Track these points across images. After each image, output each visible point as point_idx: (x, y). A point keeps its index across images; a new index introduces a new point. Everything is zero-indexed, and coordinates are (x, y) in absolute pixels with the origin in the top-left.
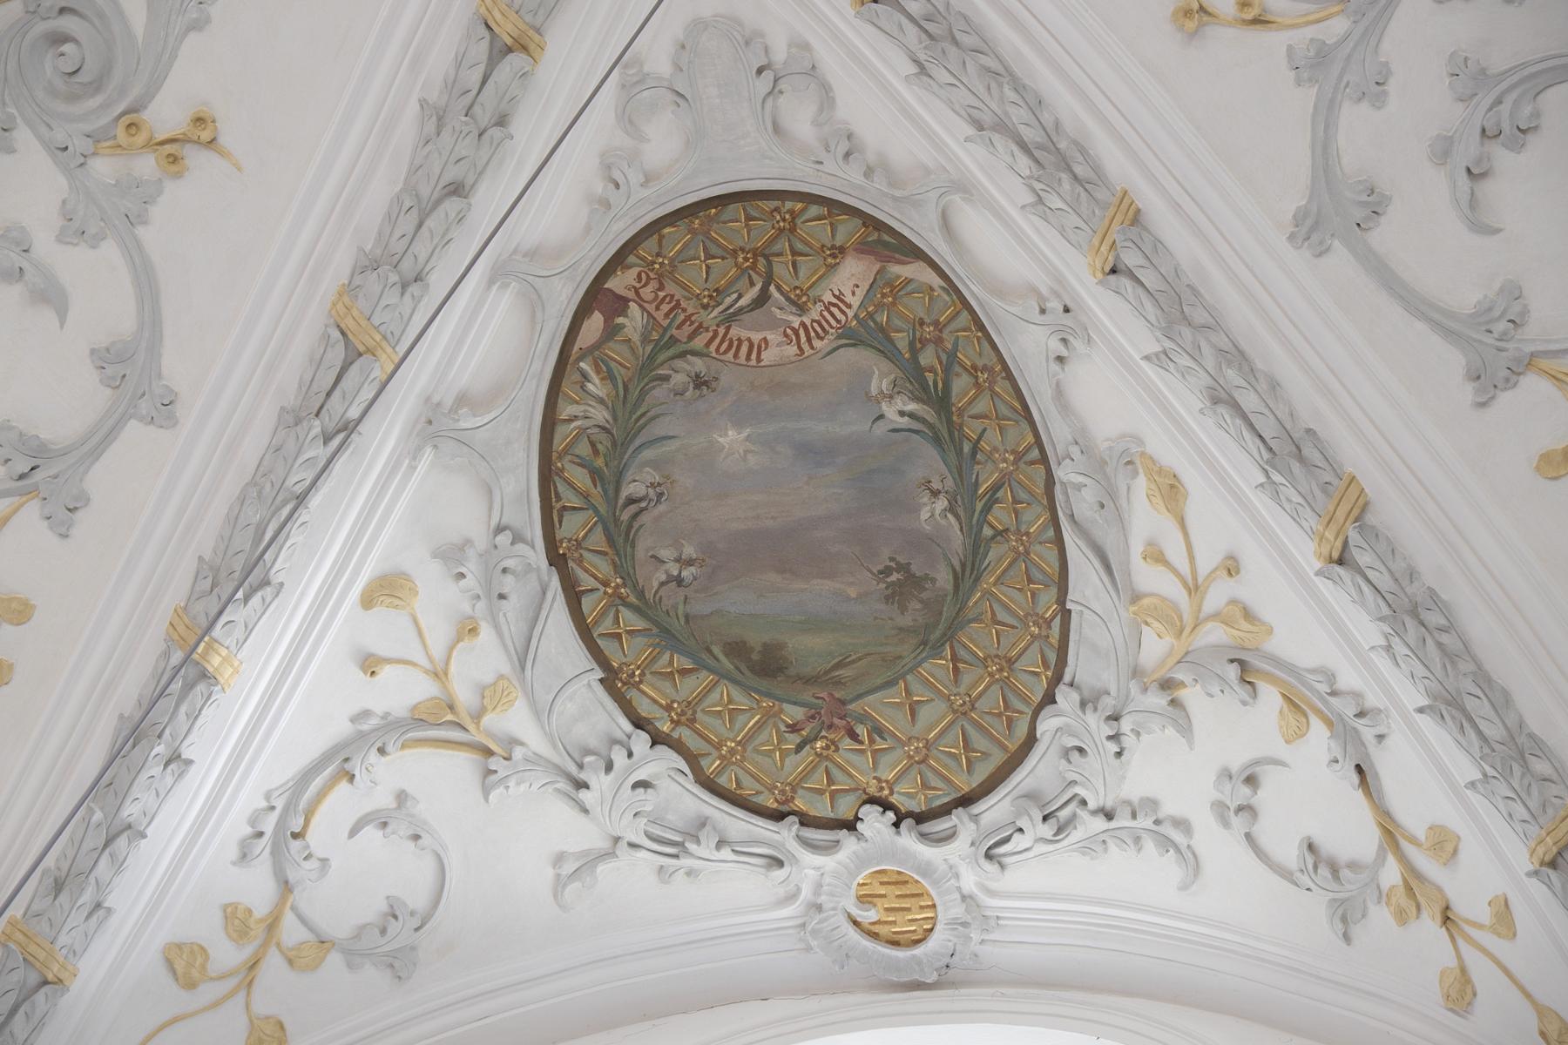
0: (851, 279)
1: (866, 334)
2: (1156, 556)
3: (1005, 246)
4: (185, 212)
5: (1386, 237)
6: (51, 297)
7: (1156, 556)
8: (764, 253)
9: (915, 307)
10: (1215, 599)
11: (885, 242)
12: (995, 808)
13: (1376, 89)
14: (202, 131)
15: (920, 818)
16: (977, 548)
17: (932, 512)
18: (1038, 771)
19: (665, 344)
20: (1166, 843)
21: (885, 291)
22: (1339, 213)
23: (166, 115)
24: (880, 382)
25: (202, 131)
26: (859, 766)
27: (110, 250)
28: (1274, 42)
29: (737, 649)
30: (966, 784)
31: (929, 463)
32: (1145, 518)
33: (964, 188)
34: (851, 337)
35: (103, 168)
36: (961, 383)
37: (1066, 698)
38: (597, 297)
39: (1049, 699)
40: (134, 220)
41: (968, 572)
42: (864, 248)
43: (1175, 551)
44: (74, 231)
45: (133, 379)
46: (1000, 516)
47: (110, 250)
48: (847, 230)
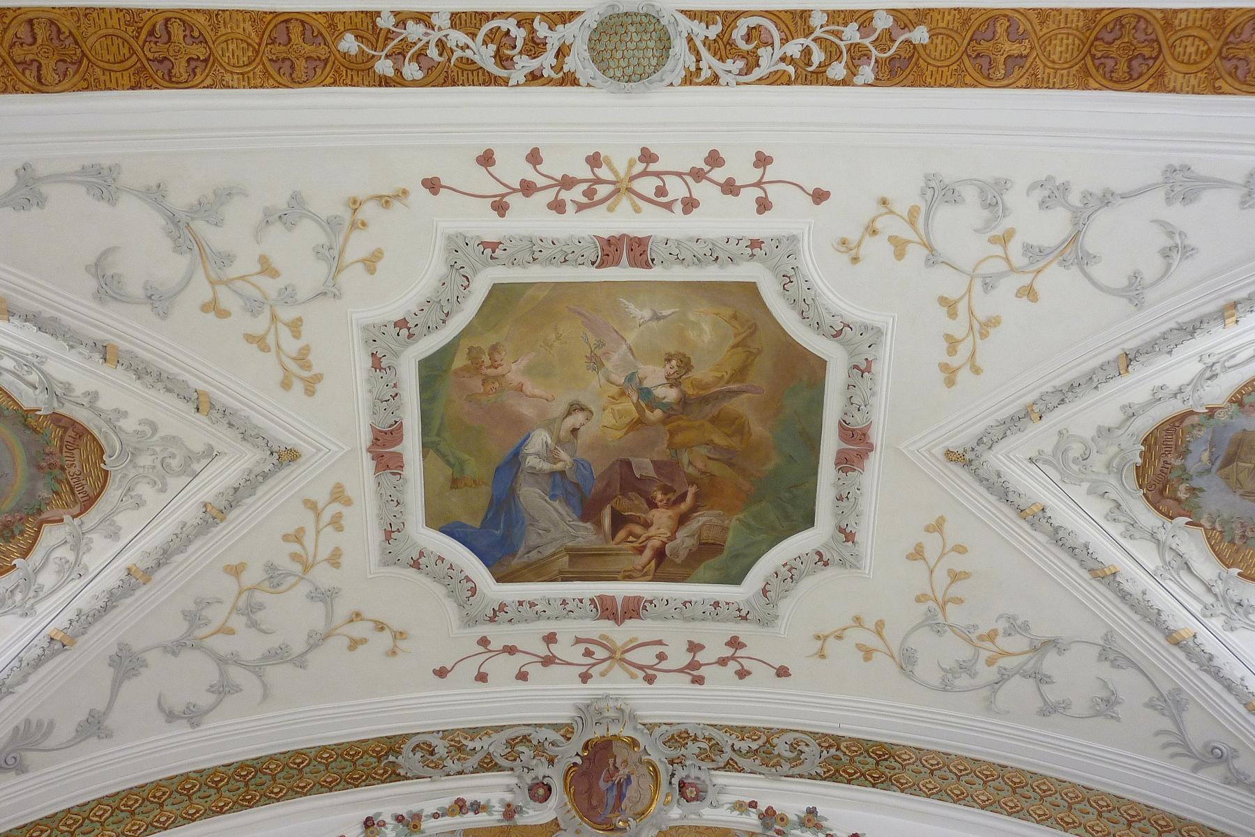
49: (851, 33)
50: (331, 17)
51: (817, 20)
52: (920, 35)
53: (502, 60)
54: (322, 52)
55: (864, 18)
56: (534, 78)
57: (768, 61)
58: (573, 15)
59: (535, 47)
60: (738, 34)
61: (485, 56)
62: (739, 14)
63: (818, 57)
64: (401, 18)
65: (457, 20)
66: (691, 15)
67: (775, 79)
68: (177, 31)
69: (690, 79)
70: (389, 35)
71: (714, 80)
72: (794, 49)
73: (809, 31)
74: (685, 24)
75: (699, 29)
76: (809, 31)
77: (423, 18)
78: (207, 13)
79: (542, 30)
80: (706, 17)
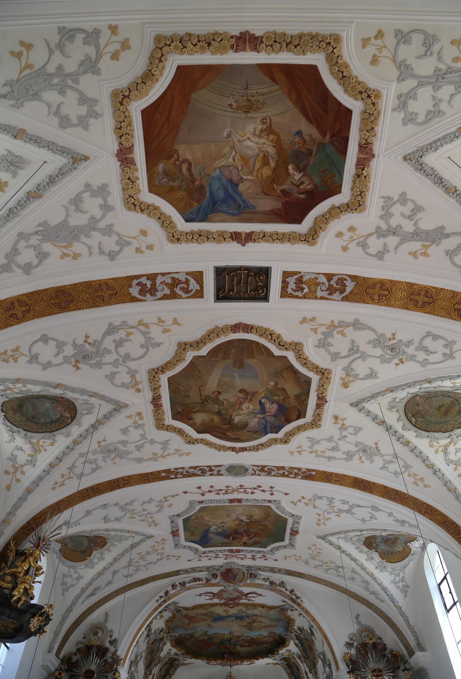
0: (67, 415)
1: (62, 416)
2: (44, 442)
3: (75, 430)
4: (69, 368)
6: (56, 355)
7: (44, 442)
8: (69, 408)
9: (66, 420)
10: (41, 448)
11: (73, 418)
12: (9, 424)
14: (78, 368)
15: (5, 417)
16: (40, 424)
17: (43, 420)
18: (15, 428)
19: (58, 401)
20: (11, 440)
21: (67, 418)
22: (81, 455)
23: (80, 365)
24: (57, 417)
25: (78, 368)
26: (10, 412)
27: (63, 361)
28: (97, 448)
29: (22, 404)
30: (11, 421)
31: (49, 420)
32: (48, 441)
33: (80, 427)
34: (61, 415)
35: (73, 360)
36: (58, 424)
37: (25, 432)
38: (62, 398)
39: (24, 430)
40: (67, 363)
41: (37, 423)
42: (71, 416)
43: (45, 444)
44: (65, 357)
45: (47, 365)
46: (44, 427)
47: (63, 361)
48: (74, 415)
49: (296, 471)
50: (159, 472)
51: (286, 468)
52: (314, 473)
53: (202, 472)
54: (157, 477)
55: (299, 469)
56: (211, 475)
57: (273, 473)
58: (221, 466)
59: (211, 470)
60: (266, 469)
61: (199, 473)
62: (266, 466)
63: (286, 473)
64: (176, 469)
65: (190, 468)
66: (254, 466)
68: (121, 481)
69: (252, 474)
70: (173, 472)
71: (259, 475)
72: (281, 472)
73: (284, 469)
74: (252, 467)
75: (255, 468)
76: (284, 469)
77: (183, 468)
79: (213, 468)
80: (258, 466)
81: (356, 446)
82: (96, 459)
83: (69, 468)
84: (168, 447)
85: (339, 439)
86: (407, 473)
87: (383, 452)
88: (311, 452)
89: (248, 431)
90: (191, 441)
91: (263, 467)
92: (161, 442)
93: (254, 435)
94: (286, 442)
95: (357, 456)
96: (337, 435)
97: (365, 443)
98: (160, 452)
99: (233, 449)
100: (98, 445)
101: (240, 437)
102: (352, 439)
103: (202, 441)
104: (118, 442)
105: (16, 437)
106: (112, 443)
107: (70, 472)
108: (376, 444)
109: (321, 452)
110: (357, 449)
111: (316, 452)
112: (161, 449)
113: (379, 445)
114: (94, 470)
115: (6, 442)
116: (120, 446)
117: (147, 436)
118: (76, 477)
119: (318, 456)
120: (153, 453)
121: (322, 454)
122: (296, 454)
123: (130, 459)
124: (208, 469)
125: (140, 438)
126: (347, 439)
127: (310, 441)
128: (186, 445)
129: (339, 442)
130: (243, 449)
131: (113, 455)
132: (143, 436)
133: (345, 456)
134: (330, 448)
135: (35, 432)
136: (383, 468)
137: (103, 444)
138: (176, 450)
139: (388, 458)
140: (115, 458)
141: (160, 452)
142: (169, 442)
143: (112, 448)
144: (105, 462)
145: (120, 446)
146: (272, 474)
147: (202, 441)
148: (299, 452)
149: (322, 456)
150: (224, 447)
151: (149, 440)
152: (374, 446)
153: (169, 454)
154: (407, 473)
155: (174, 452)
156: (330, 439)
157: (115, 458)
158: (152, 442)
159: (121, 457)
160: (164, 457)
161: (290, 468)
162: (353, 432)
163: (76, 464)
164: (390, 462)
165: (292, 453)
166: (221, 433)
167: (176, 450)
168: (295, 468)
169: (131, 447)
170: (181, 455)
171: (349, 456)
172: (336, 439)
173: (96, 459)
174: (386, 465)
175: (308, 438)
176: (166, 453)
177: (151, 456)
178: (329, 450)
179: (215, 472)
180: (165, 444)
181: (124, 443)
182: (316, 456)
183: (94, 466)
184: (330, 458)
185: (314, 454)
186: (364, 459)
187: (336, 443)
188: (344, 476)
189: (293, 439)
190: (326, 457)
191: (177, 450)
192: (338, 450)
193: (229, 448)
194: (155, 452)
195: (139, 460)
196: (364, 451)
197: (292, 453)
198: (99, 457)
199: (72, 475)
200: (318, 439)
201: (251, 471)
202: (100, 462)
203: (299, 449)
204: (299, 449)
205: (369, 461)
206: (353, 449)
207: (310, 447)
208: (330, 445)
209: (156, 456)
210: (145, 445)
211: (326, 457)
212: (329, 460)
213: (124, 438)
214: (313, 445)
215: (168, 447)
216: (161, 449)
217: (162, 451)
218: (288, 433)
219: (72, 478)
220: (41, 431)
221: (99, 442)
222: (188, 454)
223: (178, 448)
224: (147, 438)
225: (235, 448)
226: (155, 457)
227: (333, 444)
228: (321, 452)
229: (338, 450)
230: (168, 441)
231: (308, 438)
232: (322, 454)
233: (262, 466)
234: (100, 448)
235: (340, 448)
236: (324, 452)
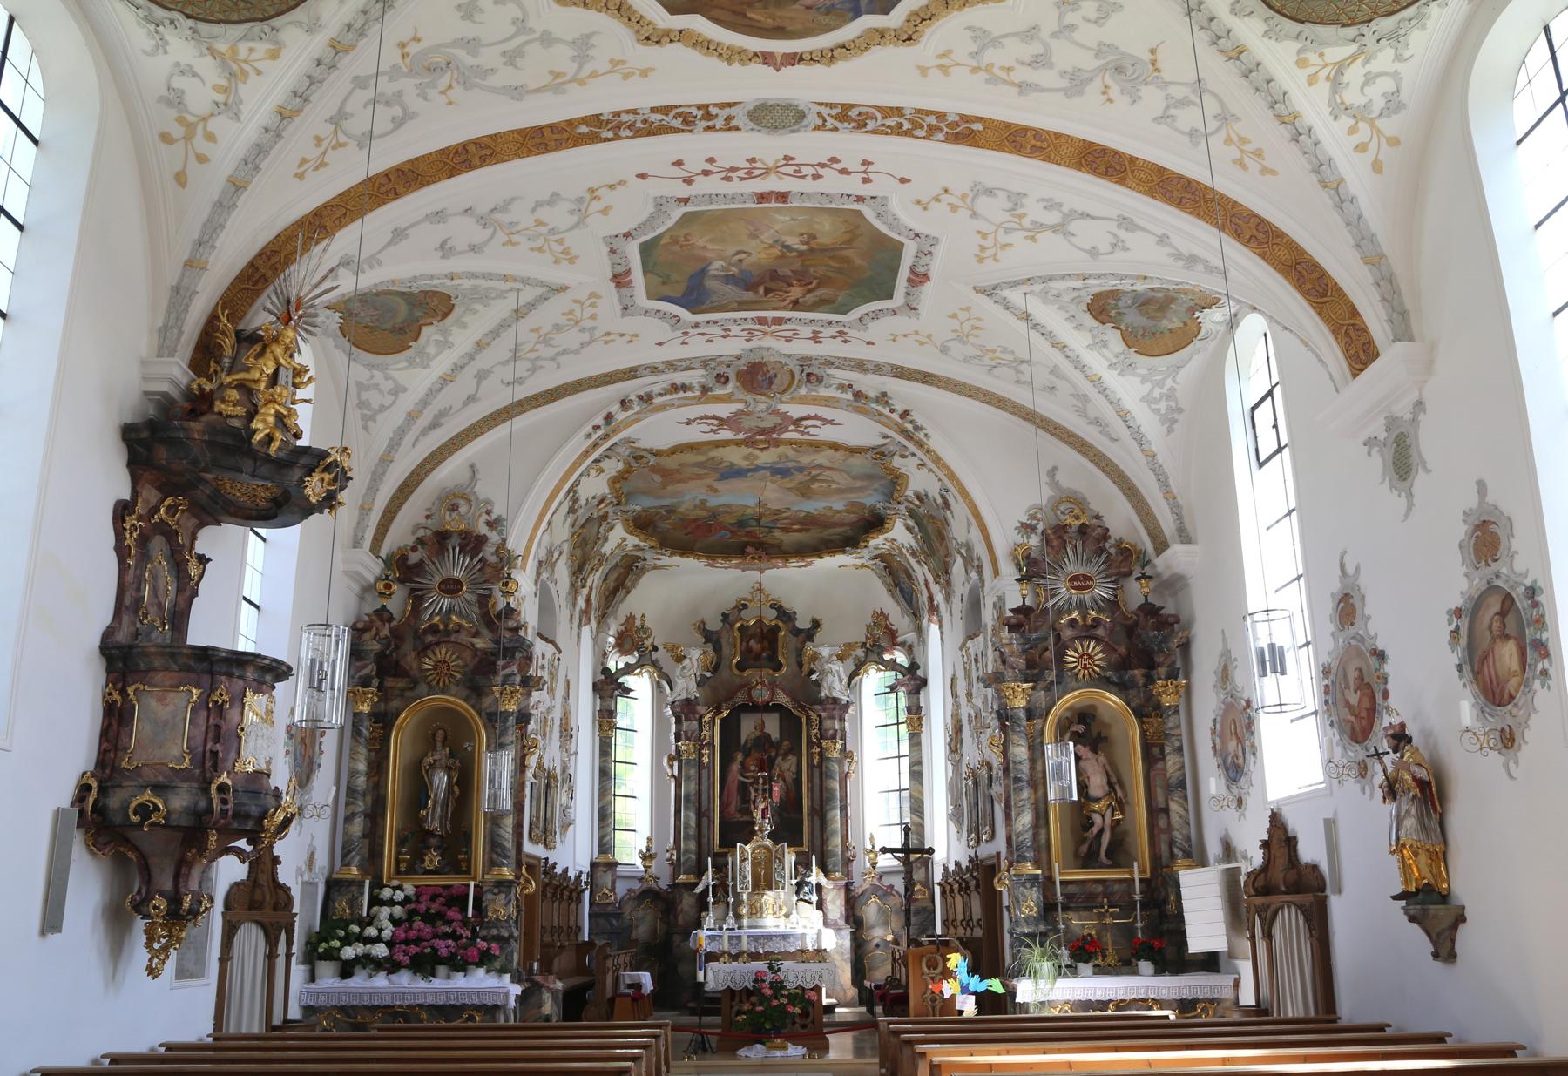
2: (251, 50)
5: (358, 91)
7: (251, 50)
13: (390, 80)
18: (159, 13)
20: (157, 46)
22: (359, 82)
32: (262, 48)
37: (190, 22)
39: (188, 17)
43: (254, 56)
49: (932, 120)
50: (569, 122)
51: (907, 112)
52: (978, 127)
53: (686, 122)
54: (566, 135)
55: (941, 116)
56: (709, 128)
57: (871, 125)
58: (735, 104)
59: (708, 116)
60: (853, 113)
61: (677, 123)
62: (853, 106)
63: (907, 126)
64: (617, 114)
65: (653, 110)
67: (875, 132)
68: (472, 148)
69: (817, 128)
70: (608, 122)
71: (836, 129)
72: (891, 122)
73: (902, 115)
75: (825, 111)
76: (902, 115)
77: (634, 112)
78: (490, 136)
79: (714, 111)
80: (832, 106)
81: (1097, 56)
82: (400, 94)
83: (331, 120)
84: (590, 53)
85: (1054, 35)
86: (1222, 134)
87: (1166, 75)
88: (975, 70)
89: (808, 8)
90: (654, 38)
91: (846, 107)
92: (570, 39)
93: (824, 19)
94: (910, 39)
95: (1097, 85)
96: (1049, 24)
97: (1123, 48)
98: (570, 68)
99: (766, 58)
100: (399, 52)
101: (786, 24)
102: (1090, 35)
103: (682, 35)
104: (455, 43)
105: (168, 37)
106: (439, 46)
107: (335, 131)
108: (1153, 52)
109: (1002, 68)
110: (1101, 62)
111: (989, 68)
112: (573, 59)
113: (1160, 56)
114: (398, 123)
115: (145, 52)
116: (460, 53)
117: (531, 23)
118: (353, 145)
119: (993, 80)
120: (551, 72)
121: (1003, 75)
122: (935, 74)
123: (491, 90)
124: (700, 113)
125: (513, 30)
126: (1076, 36)
127: (975, 38)
128: (639, 47)
129: (1054, 43)
130: (795, 59)
131: (445, 81)
132: (521, 25)
133: (1065, 83)
134: (1027, 59)
135: (218, 22)
136: (1164, 118)
137: (413, 49)
138: (611, 61)
139: (1178, 92)
140: (450, 87)
141: (570, 68)
142: (594, 41)
143: (440, 60)
144: (425, 99)
145: (460, 53)
146: (869, 127)
147: (682, 35)
148: (944, 69)
149: (1005, 82)
150: (741, 52)
151: (536, 35)
152: (1147, 57)
153: (594, 74)
154: (1222, 134)
155: (608, 67)
156: (1030, 34)
157: (450, 87)
158: (547, 40)
159: (466, 84)
160: (582, 82)
161: (918, 111)
162: (1093, 15)
163: (349, 108)
164: (1184, 103)
165: (923, 71)
166: (734, 12)
167: (611, 61)
168: (929, 113)
169: (489, 57)
170: (626, 77)
171: (1076, 83)
172: (1045, 33)
173: (400, 94)
174: (1172, 111)
175: (969, 28)
176: (586, 71)
177: (547, 79)
178: (1023, 64)
179: (719, 123)
180: (583, 45)
181: (472, 45)
182: (988, 81)
183: (397, 111)
184: (1024, 88)
185: (983, 75)
186: (1114, 92)
187: (1046, 45)
188: (1058, 135)
189: (928, 31)
190: (1013, 84)
191: (615, 63)
192: (1049, 65)
193: (756, 55)
194: (557, 69)
195: (517, 92)
196: (1119, 70)
197: (923, 71)
198: (408, 85)
199: (342, 138)
200: (996, 33)
201: (812, 119)
202: (413, 101)
203: (945, 61)
204: (945, 61)
205: (1127, 99)
206: (1089, 62)
207: (974, 55)
208: (1029, 50)
209: (559, 80)
210: (527, 48)
211: (1013, 84)
212: (1020, 93)
213: (468, 30)
214: (983, 47)
215: (590, 53)
216: (573, 59)
217: (575, 66)
218: (916, 14)
219: (344, 145)
220: (235, 18)
221: (403, 45)
222: (644, 73)
223: (618, 57)
224: (532, 31)
225: (772, 54)
226: (557, 83)
227: (1036, 48)
228: (1002, 68)
229: (1049, 65)
230: (589, 36)
231: (969, 28)
232: (1003, 75)
233: (843, 105)
234: (408, 60)
235: (1054, 60)
236: (1009, 69)
